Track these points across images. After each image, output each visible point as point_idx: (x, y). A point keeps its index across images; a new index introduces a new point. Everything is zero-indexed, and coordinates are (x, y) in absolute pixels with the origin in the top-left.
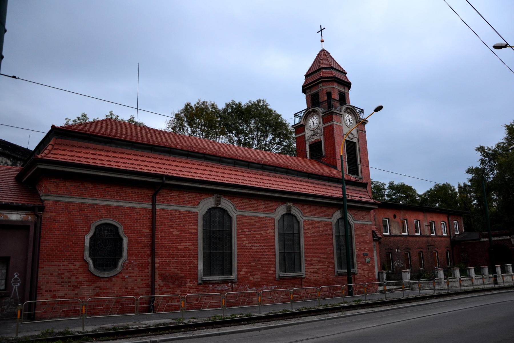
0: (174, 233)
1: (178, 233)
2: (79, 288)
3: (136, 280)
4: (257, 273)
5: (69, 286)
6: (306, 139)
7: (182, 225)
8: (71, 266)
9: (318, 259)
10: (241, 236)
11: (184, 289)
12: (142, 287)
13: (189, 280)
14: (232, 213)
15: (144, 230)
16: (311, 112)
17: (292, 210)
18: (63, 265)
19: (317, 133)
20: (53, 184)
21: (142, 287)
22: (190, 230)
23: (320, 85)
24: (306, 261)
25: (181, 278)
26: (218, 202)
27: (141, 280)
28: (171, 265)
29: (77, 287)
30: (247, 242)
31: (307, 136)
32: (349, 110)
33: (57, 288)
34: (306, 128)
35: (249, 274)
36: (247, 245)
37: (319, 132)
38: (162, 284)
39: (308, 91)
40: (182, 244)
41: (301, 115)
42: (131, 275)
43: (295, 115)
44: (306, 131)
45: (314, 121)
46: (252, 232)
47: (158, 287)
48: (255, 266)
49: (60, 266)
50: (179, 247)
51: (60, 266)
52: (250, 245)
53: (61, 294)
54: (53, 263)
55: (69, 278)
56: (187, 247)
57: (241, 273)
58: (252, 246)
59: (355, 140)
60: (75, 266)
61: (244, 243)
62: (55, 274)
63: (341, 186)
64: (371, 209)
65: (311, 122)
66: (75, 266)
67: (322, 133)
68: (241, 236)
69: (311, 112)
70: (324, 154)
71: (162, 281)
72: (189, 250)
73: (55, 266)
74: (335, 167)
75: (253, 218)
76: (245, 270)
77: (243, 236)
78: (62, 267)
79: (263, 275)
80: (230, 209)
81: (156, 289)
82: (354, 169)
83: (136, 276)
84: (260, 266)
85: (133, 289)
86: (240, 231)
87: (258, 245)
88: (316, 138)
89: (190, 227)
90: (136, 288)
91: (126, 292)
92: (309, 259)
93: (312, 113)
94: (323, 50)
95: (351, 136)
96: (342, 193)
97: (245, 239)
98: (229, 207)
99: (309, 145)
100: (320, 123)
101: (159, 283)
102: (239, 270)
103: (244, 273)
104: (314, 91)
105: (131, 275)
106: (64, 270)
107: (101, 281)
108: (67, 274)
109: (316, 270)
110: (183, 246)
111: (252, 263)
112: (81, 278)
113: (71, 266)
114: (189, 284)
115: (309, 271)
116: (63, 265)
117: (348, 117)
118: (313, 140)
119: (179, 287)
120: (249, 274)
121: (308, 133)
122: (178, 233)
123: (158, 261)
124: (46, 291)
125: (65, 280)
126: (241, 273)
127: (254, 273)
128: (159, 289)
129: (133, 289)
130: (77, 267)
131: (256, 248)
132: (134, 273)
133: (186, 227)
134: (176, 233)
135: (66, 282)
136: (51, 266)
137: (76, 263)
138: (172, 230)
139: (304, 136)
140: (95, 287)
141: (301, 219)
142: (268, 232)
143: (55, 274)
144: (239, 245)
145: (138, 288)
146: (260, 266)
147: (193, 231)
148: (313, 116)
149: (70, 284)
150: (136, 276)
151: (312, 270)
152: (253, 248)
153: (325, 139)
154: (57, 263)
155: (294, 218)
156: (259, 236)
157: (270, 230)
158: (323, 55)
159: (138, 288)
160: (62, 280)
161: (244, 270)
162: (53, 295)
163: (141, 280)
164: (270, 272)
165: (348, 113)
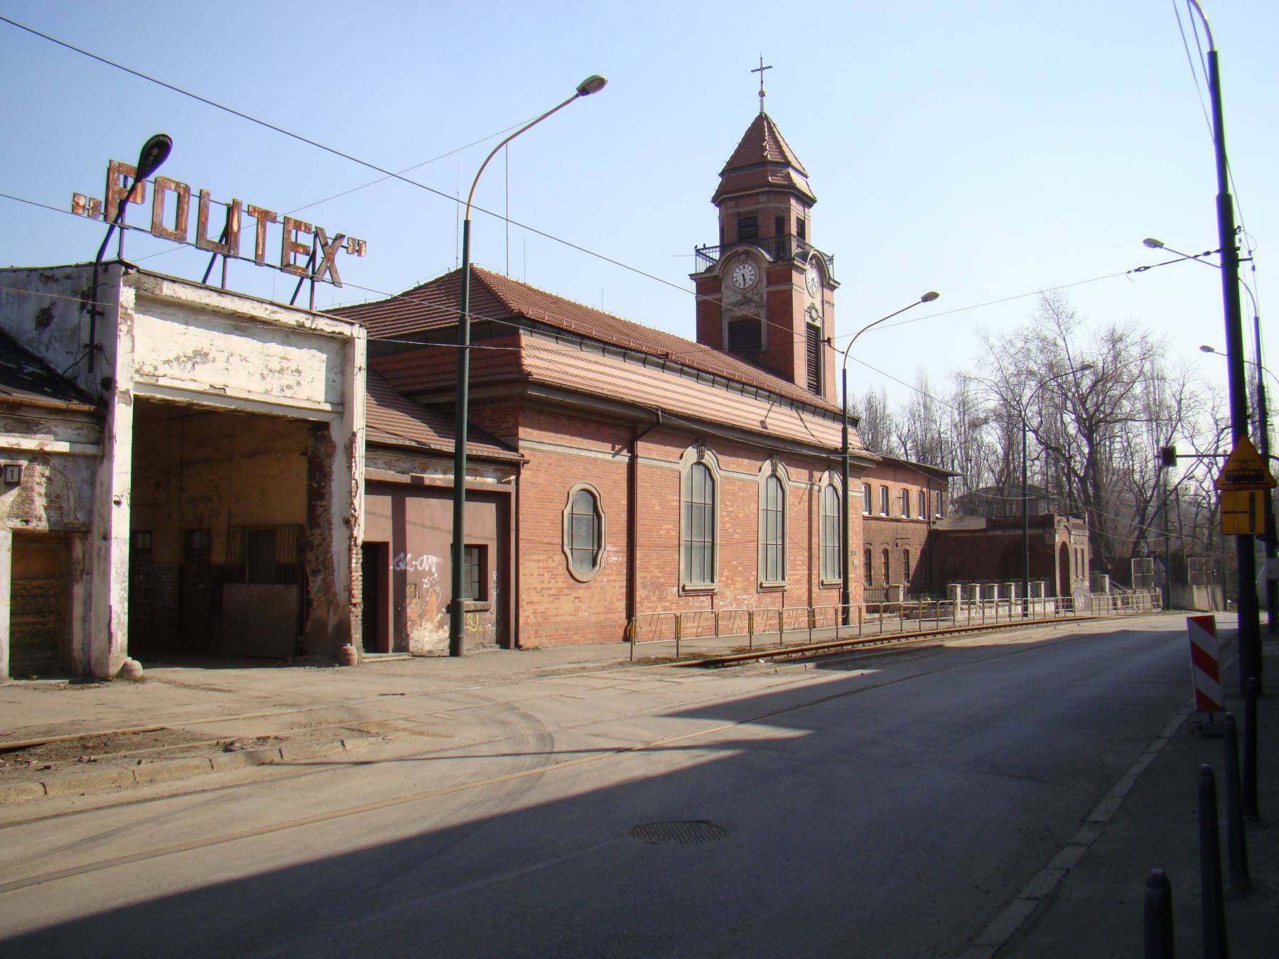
23: (763, 199)
25: (662, 584)
26: (701, 456)
28: (653, 562)
37: (756, 298)
39: (732, 203)
43: (698, 252)
45: (744, 274)
53: (541, 608)
59: (818, 324)
64: (864, 468)
70: (764, 348)
74: (790, 378)
78: (541, 564)
82: (817, 385)
88: (747, 311)
93: (743, 257)
100: (760, 281)
104: (746, 208)
117: (812, 274)
121: (728, 297)
125: (546, 585)
148: (744, 262)
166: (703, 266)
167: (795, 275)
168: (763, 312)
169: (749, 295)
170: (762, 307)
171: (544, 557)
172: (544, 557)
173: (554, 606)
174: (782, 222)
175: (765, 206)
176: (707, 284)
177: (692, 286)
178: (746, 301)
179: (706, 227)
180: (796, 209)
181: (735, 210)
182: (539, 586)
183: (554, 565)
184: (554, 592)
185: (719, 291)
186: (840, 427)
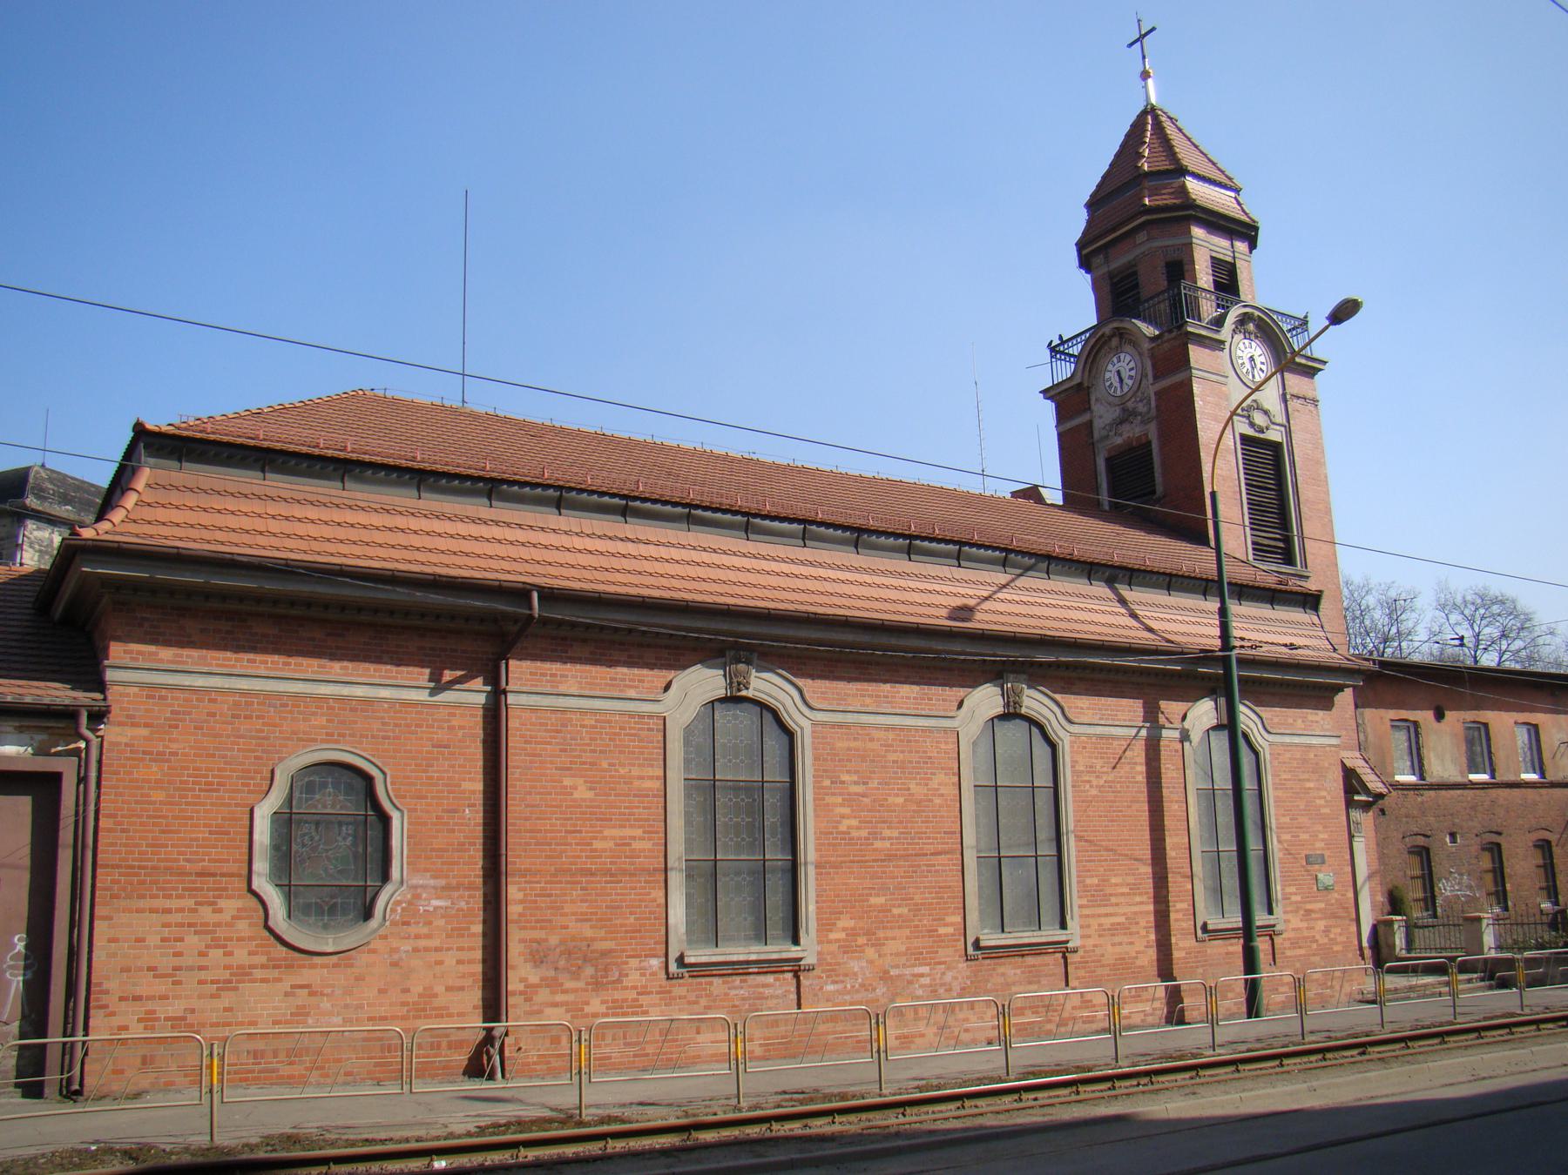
0: (576, 795)
1: (589, 795)
2: (236, 989)
3: (440, 963)
4: (890, 933)
5: (201, 982)
6: (1096, 435)
7: (605, 765)
8: (206, 914)
9: (1130, 879)
10: (829, 799)
11: (618, 995)
12: (462, 989)
13: (634, 963)
14: (797, 716)
15: (466, 785)
16: (1110, 337)
17: (1026, 702)
18: (181, 910)
19: (1134, 413)
20: (141, 625)
21: (462, 989)
22: (637, 783)
23: (1141, 237)
24: (1084, 889)
27: (459, 962)
28: (568, 908)
29: (226, 986)
30: (854, 822)
31: (1098, 424)
32: (1251, 327)
33: (162, 987)
34: (1093, 399)
35: (861, 940)
36: (855, 834)
37: (1141, 408)
38: (534, 979)
40: (607, 832)
41: (1075, 350)
42: (422, 943)
43: (1053, 350)
44: (1095, 407)
45: (1121, 370)
46: (874, 784)
47: (521, 987)
48: (885, 910)
49: (169, 911)
50: (598, 845)
51: (169, 911)
52: (864, 833)
53: (175, 1008)
54: (142, 904)
55: (202, 954)
56: (623, 843)
57: (833, 936)
58: (875, 835)
59: (1275, 435)
60: (220, 911)
61: (843, 828)
62: (152, 940)
63: (1213, 605)
65: (1110, 375)
66: (220, 911)
67: (1153, 412)
68: (829, 799)
69: (1110, 337)
70: (1160, 489)
71: (536, 966)
72: (634, 855)
73: (152, 911)
75: (876, 734)
76: (845, 922)
77: (839, 800)
78: (177, 918)
79: (917, 943)
80: (789, 703)
81: (514, 993)
83: (437, 949)
84: (905, 910)
85: (429, 994)
86: (827, 783)
87: (895, 834)
88: (1131, 431)
89: (636, 772)
90: (440, 989)
91: (404, 1004)
92: (1095, 881)
93: (1115, 342)
94: (1150, 111)
95: (1259, 419)
96: (1217, 632)
97: (847, 811)
98: (782, 696)
99: (1108, 460)
100: (1144, 375)
101: (523, 973)
102: (825, 926)
103: (842, 935)
104: (1119, 261)
105: (422, 943)
106: (181, 925)
107: (313, 966)
108: (193, 941)
109: (1121, 919)
110: (613, 838)
111: (874, 900)
112: (241, 956)
113: (206, 914)
114: (634, 978)
115: (1094, 922)
116: (181, 910)
118: (1119, 441)
119: (597, 985)
120: (861, 940)
121: (1102, 414)
122: (589, 795)
123: (520, 896)
124: (121, 999)
126: (833, 936)
127: (881, 934)
128: (521, 993)
129: (429, 994)
130: (226, 917)
131: (887, 844)
132: (428, 937)
133: (622, 771)
134: (583, 793)
135: (191, 968)
136: (138, 911)
137: (222, 903)
138: (567, 782)
139: (1090, 424)
140: (293, 987)
141: (1061, 733)
142: (934, 784)
143: (152, 940)
144: (821, 834)
145: (448, 989)
146: (905, 910)
147: (648, 784)
148: (1118, 350)
149: (203, 975)
150: (437, 949)
151: (1107, 921)
152: (878, 844)
153: (1161, 436)
154: (159, 903)
155: (1035, 730)
156: (900, 800)
157: (940, 777)
158: (1148, 126)
159: (448, 989)
160: (177, 961)
161: (840, 924)
162: (147, 1012)
163: (459, 962)
164: (942, 930)
165: (1247, 335)
166: (1065, 370)
167: (1196, 354)
168: (1152, 431)
169: (1130, 405)
170: (1149, 421)
171: (190, 903)
172: (190, 903)
173: (227, 1000)
174: (1179, 269)
175: (1143, 249)
176: (1069, 400)
177: (1049, 408)
178: (1127, 416)
179: (1075, 306)
180: (1206, 246)
181: (1104, 270)
182: (166, 963)
183: (226, 917)
184: (226, 975)
185: (1087, 408)
186: (1213, 605)
